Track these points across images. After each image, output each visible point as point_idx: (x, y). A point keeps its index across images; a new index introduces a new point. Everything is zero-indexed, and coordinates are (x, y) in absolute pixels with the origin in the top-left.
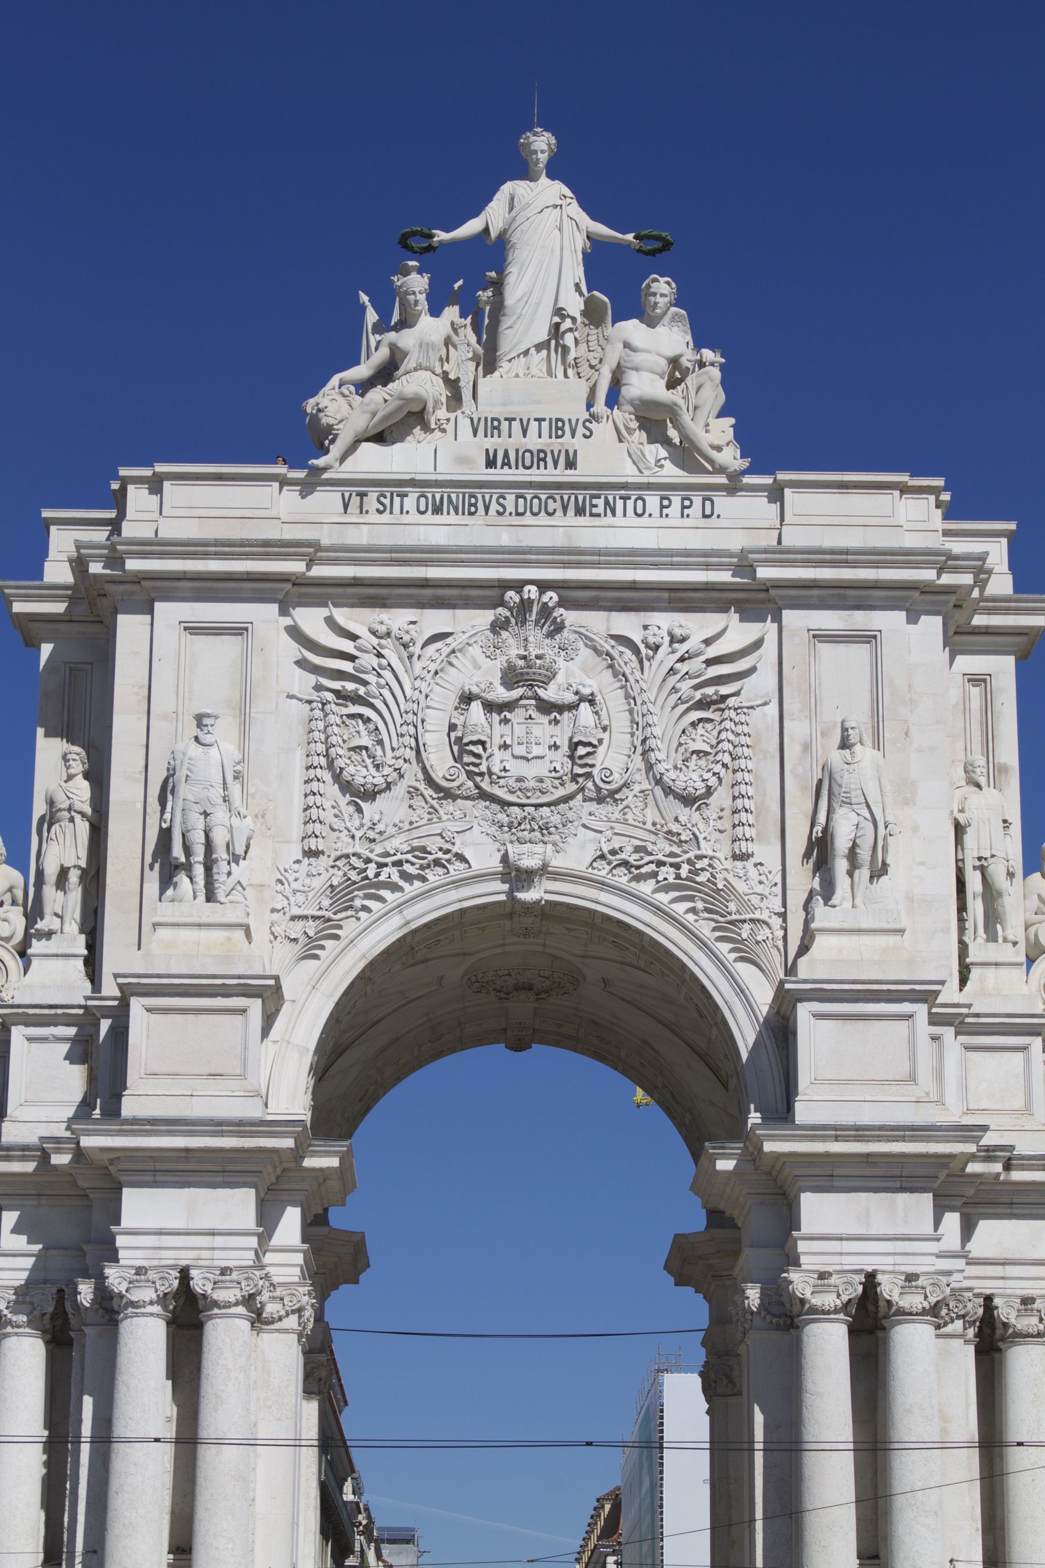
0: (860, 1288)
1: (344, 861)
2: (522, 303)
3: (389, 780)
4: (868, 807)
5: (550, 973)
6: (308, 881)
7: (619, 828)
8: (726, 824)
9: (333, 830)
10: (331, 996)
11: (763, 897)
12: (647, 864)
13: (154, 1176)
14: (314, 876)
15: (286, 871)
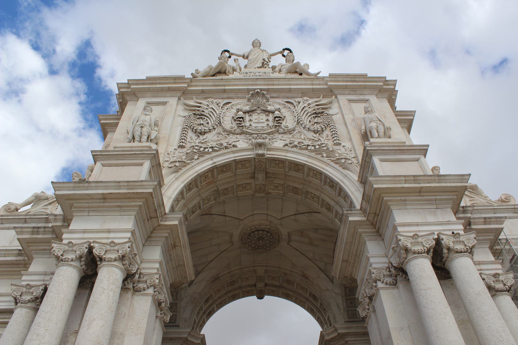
0: (434, 242)
1: (192, 148)
2: (254, 59)
3: (210, 128)
4: (380, 121)
5: (270, 227)
6: (179, 154)
7: (292, 139)
8: (330, 137)
9: (189, 142)
10: (183, 182)
11: (347, 154)
12: (303, 146)
13: (89, 212)
14: (181, 153)
15: (171, 152)
